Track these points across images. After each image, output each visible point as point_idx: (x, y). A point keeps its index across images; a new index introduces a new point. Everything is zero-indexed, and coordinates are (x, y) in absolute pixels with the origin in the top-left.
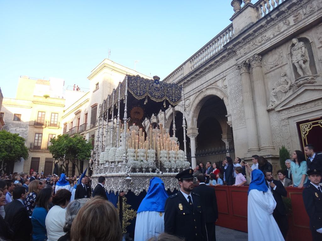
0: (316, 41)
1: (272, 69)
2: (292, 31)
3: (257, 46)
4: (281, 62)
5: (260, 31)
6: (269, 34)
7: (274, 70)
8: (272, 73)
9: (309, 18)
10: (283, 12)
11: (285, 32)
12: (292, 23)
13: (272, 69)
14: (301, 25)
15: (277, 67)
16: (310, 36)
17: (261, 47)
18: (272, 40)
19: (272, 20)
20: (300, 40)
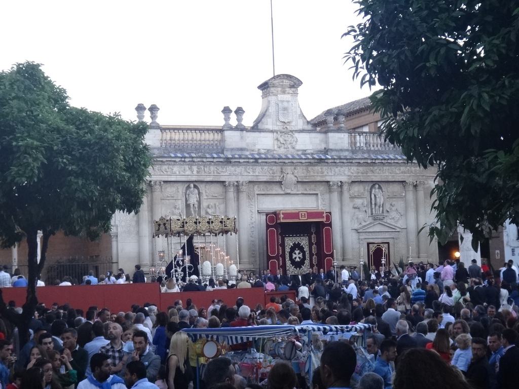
0: (204, 192)
1: (169, 198)
2: (194, 178)
3: (162, 173)
4: (176, 196)
5: (170, 163)
6: (176, 169)
7: (169, 200)
8: (167, 201)
9: (208, 177)
10: (194, 161)
11: (189, 177)
12: (195, 172)
13: (169, 198)
14: (201, 178)
15: (172, 198)
16: (202, 187)
17: (167, 176)
18: (178, 177)
19: (184, 161)
20: (195, 187)
